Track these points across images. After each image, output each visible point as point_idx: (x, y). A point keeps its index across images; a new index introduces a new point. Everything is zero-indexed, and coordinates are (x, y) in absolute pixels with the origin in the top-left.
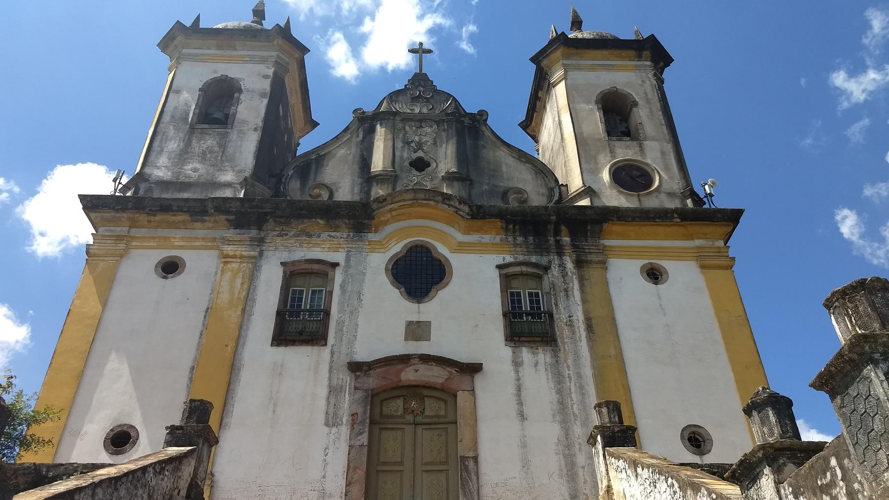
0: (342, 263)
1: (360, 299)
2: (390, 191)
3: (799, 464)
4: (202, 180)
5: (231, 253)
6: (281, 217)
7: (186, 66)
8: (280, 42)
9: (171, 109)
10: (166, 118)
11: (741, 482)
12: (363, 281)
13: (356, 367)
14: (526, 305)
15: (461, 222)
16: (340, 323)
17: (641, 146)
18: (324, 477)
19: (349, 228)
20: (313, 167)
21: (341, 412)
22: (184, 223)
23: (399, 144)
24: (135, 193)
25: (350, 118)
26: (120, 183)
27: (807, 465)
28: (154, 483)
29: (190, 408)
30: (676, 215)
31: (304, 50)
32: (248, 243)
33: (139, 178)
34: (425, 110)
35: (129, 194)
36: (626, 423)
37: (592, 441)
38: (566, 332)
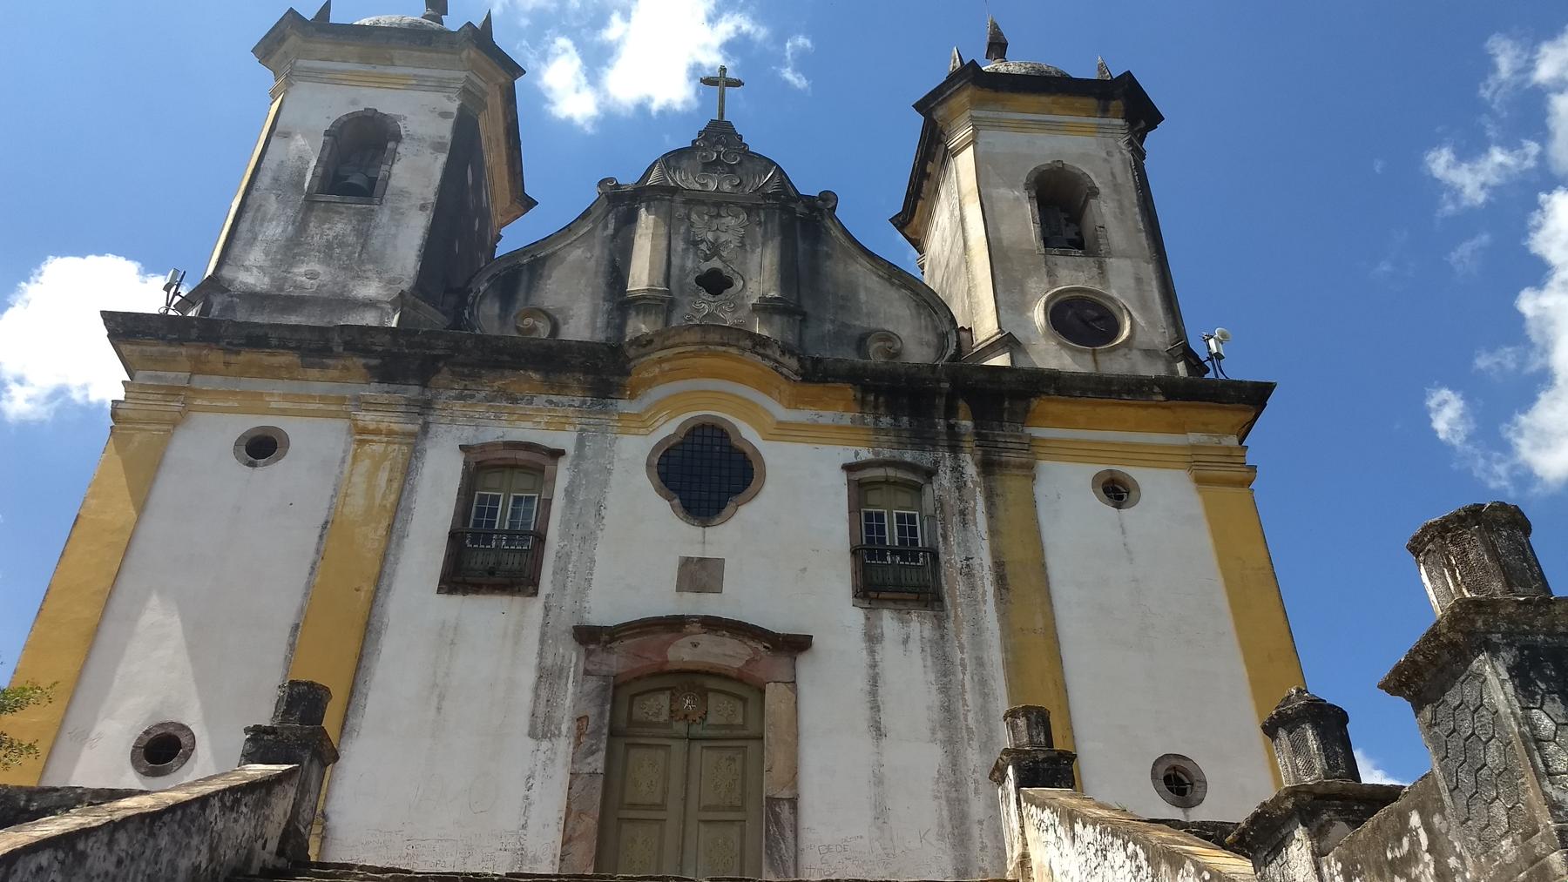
0: (570, 450)
1: (599, 516)
2: (659, 326)
3: (1356, 823)
4: (325, 293)
5: (372, 426)
6: (464, 365)
7: (303, 90)
8: (473, 55)
9: (274, 166)
10: (265, 180)
11: (1255, 852)
12: (606, 483)
13: (587, 636)
14: (892, 536)
15: (785, 386)
16: (563, 557)
17: (1101, 266)
18: (524, 827)
19: (584, 390)
20: (525, 278)
21: (558, 714)
22: (288, 367)
23: (679, 245)
24: (204, 311)
25: (593, 194)
26: (176, 293)
27: (1369, 824)
28: (220, 825)
29: (290, 695)
30: (1157, 389)
31: (516, 70)
32: (403, 409)
33: (213, 285)
34: (726, 187)
35: (192, 314)
36: (1058, 746)
37: (998, 775)
38: (961, 586)
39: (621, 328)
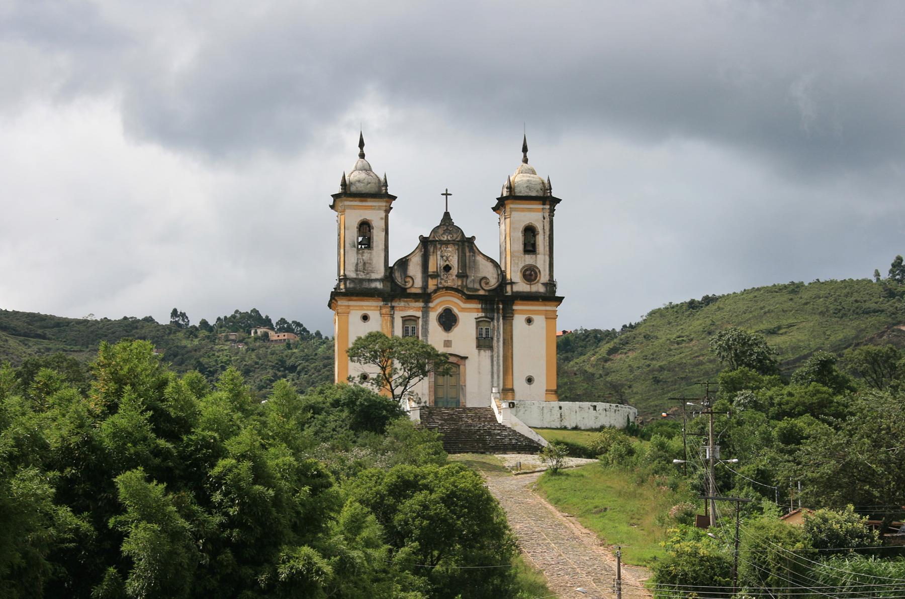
10: (347, 245)
23: (439, 257)
33: (344, 279)
39: (427, 282)
